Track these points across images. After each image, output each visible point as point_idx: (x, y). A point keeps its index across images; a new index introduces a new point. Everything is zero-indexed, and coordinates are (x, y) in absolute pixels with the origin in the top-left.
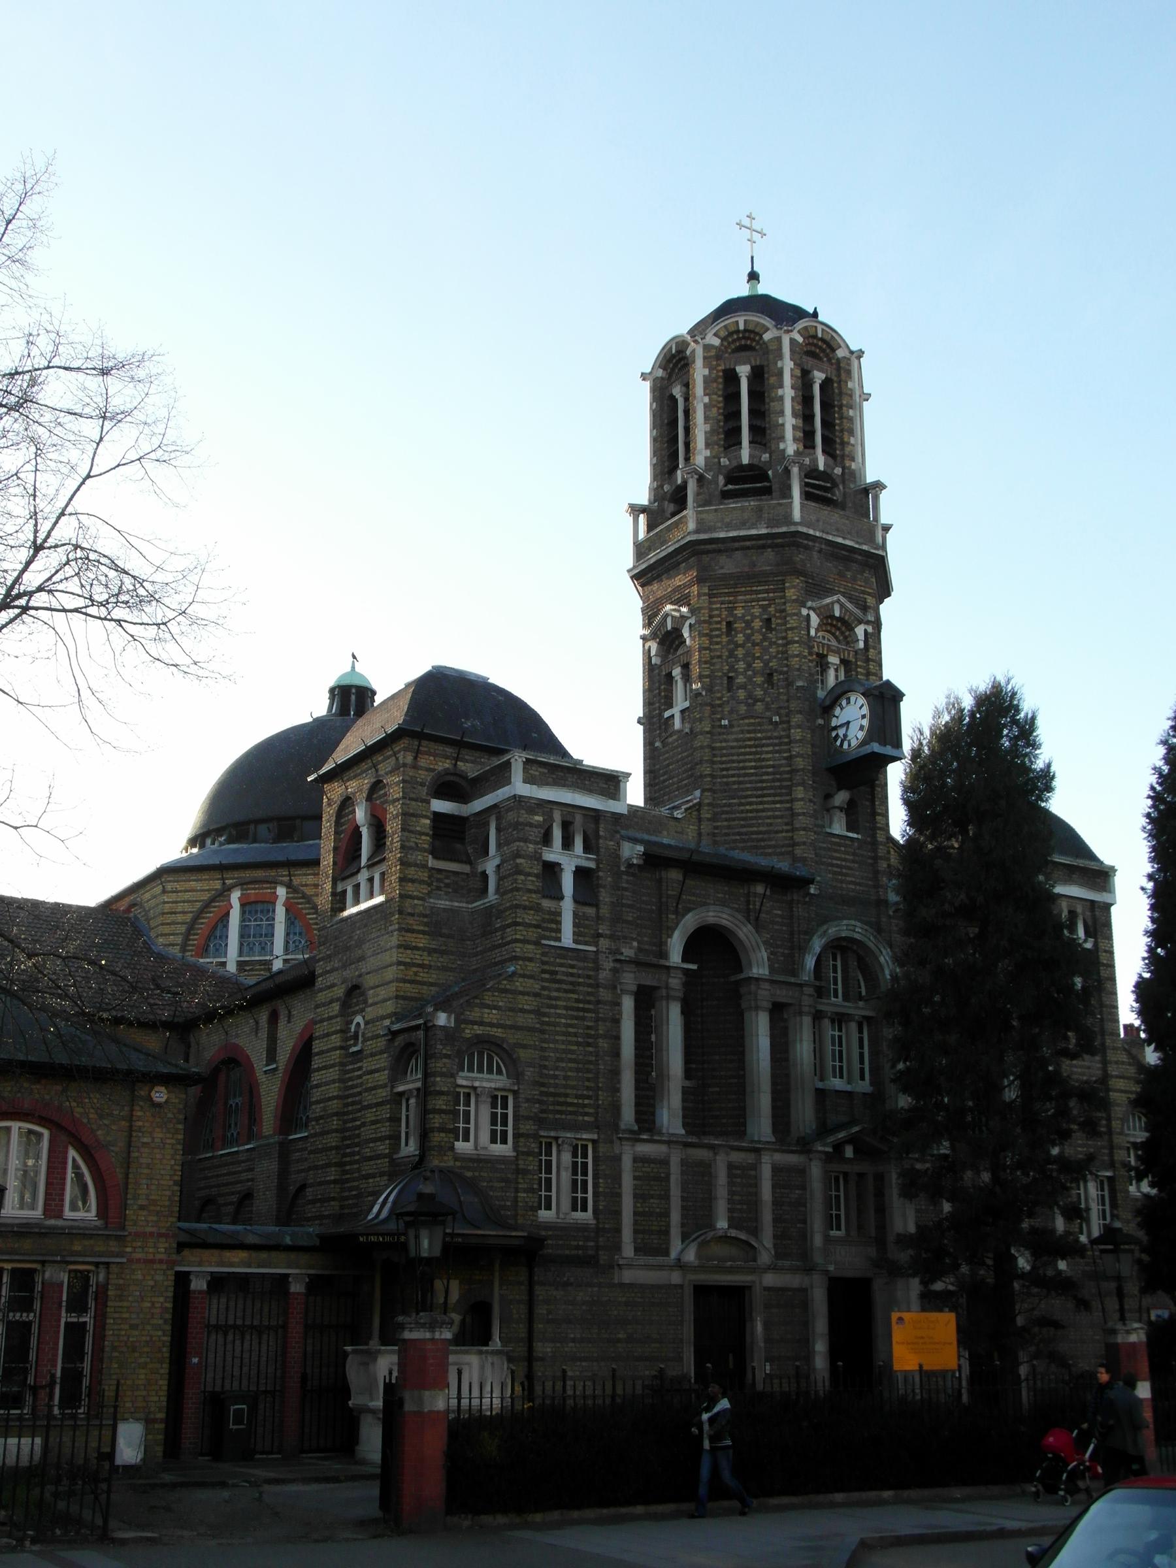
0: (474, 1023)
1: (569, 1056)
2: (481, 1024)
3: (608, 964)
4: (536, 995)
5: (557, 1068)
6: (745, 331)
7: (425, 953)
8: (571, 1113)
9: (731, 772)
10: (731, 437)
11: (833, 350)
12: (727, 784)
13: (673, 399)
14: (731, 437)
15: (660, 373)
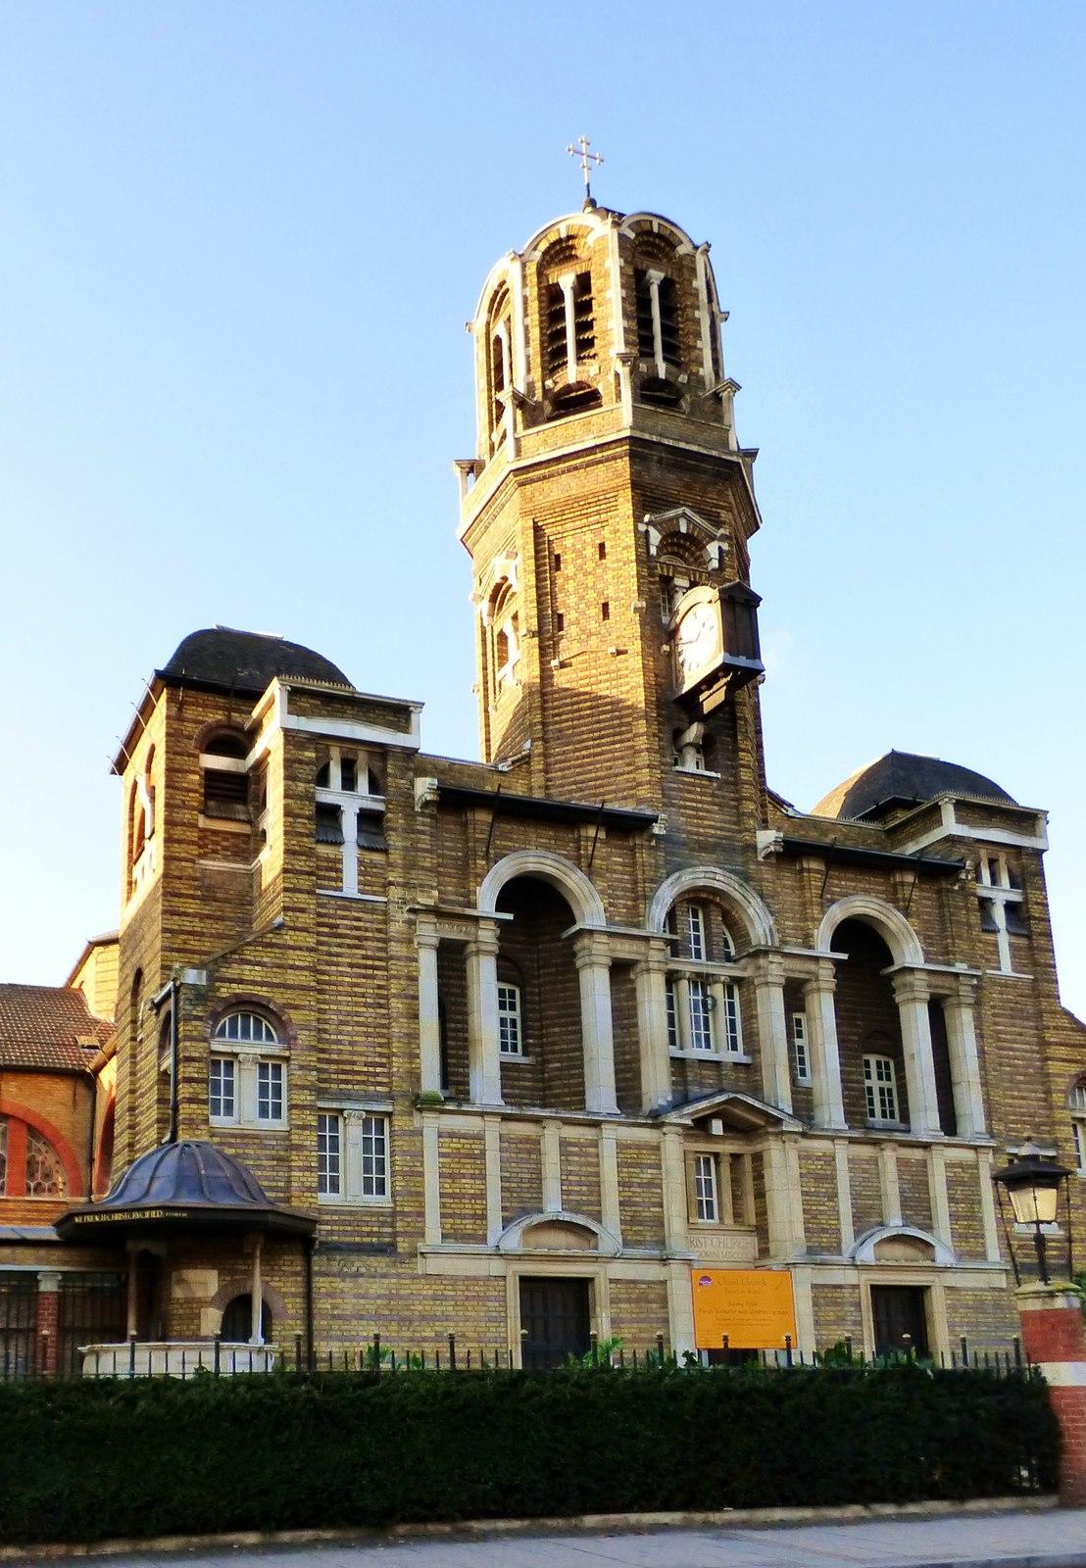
0: (232, 981)
1: (356, 1019)
2: (241, 982)
3: (400, 916)
4: (310, 950)
5: (340, 1033)
7: (197, 920)
8: (359, 1082)
9: (564, 717)
11: (673, 247)
12: (560, 731)
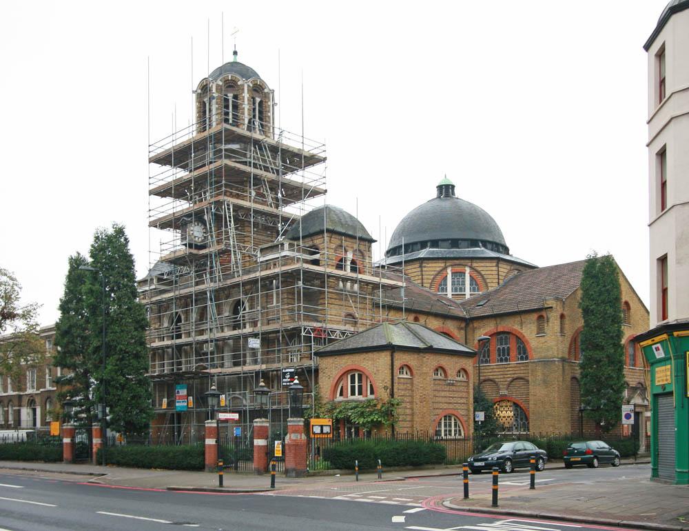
6: (231, 80)
11: (263, 89)
13: (204, 104)
15: (199, 91)
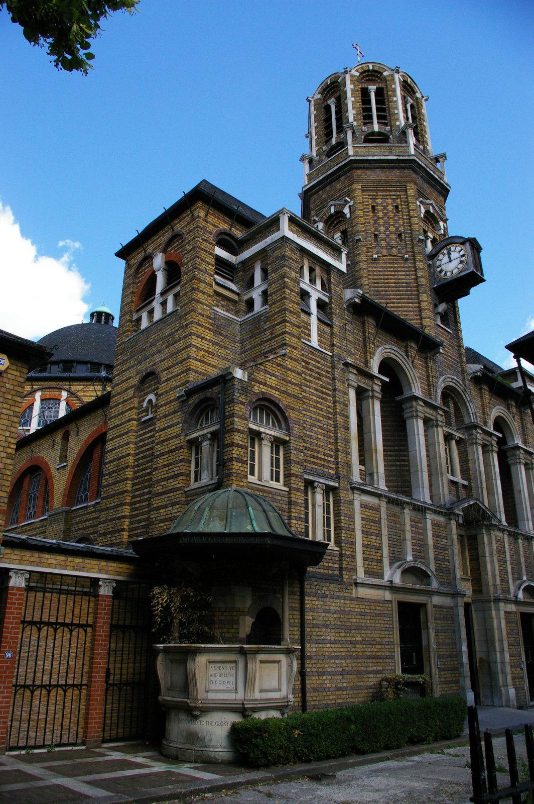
0: (261, 383)
2: (265, 384)
4: (299, 374)
9: (380, 285)
10: (368, 118)
12: (378, 291)
14: (368, 118)
